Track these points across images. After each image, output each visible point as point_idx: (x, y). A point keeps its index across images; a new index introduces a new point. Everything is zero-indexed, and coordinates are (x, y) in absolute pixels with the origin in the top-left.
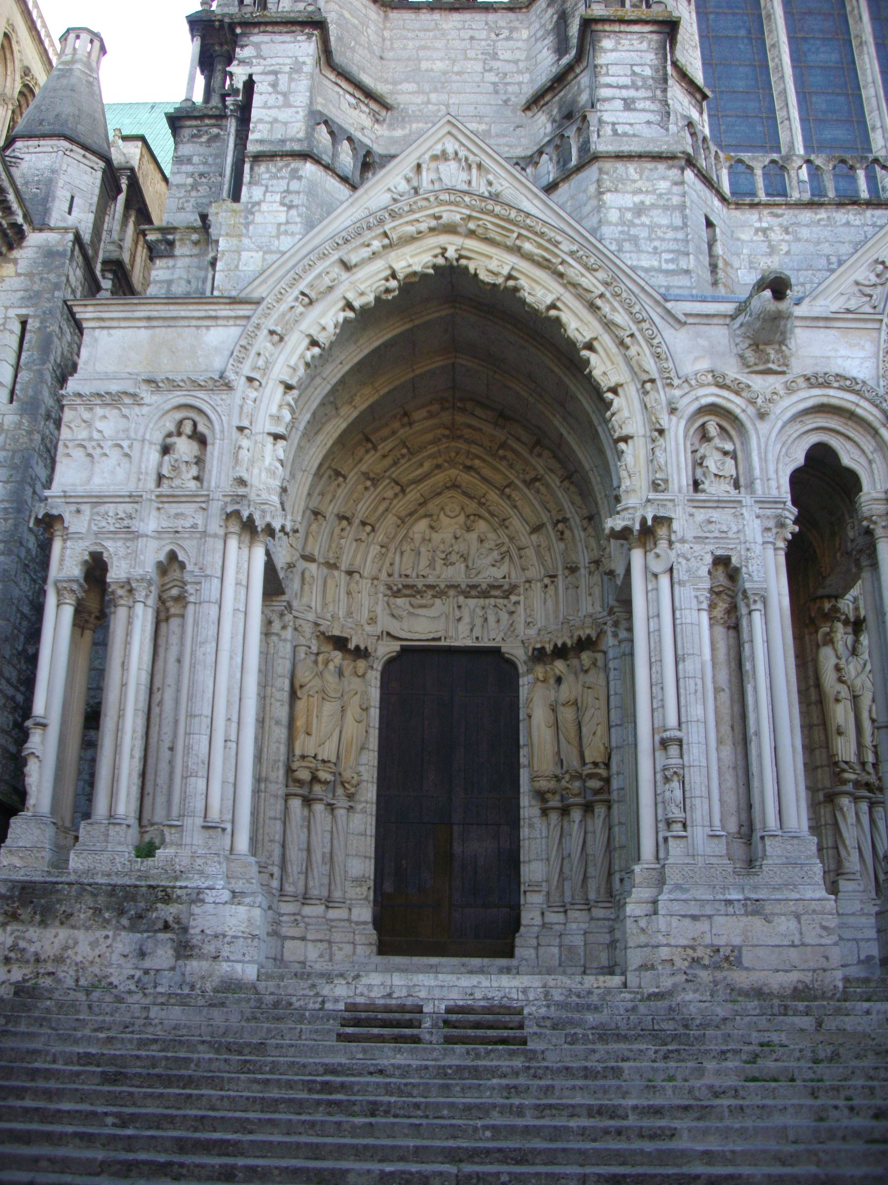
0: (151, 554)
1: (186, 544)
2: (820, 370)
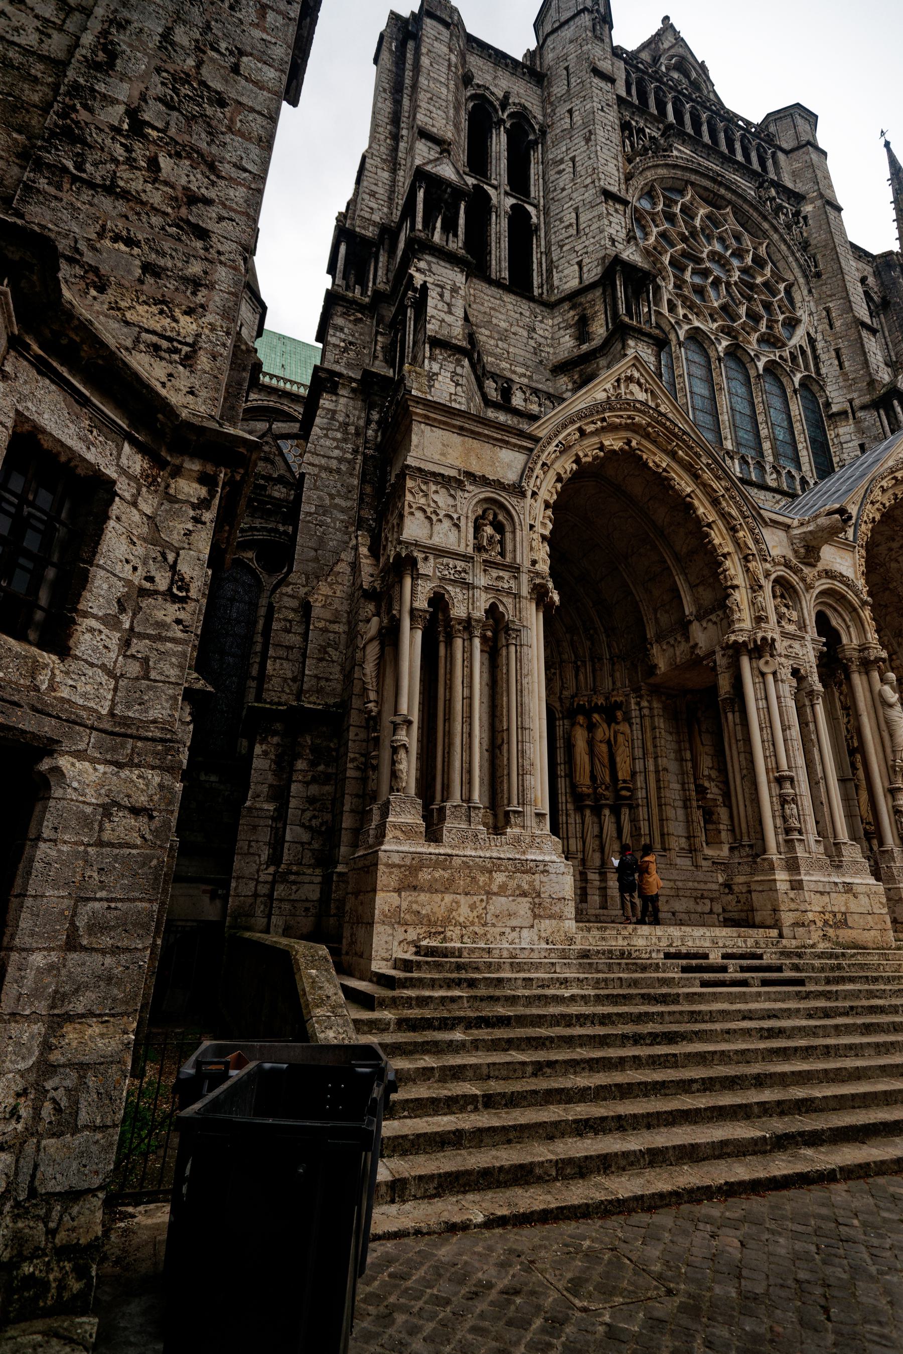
0: (483, 602)
1: (505, 600)
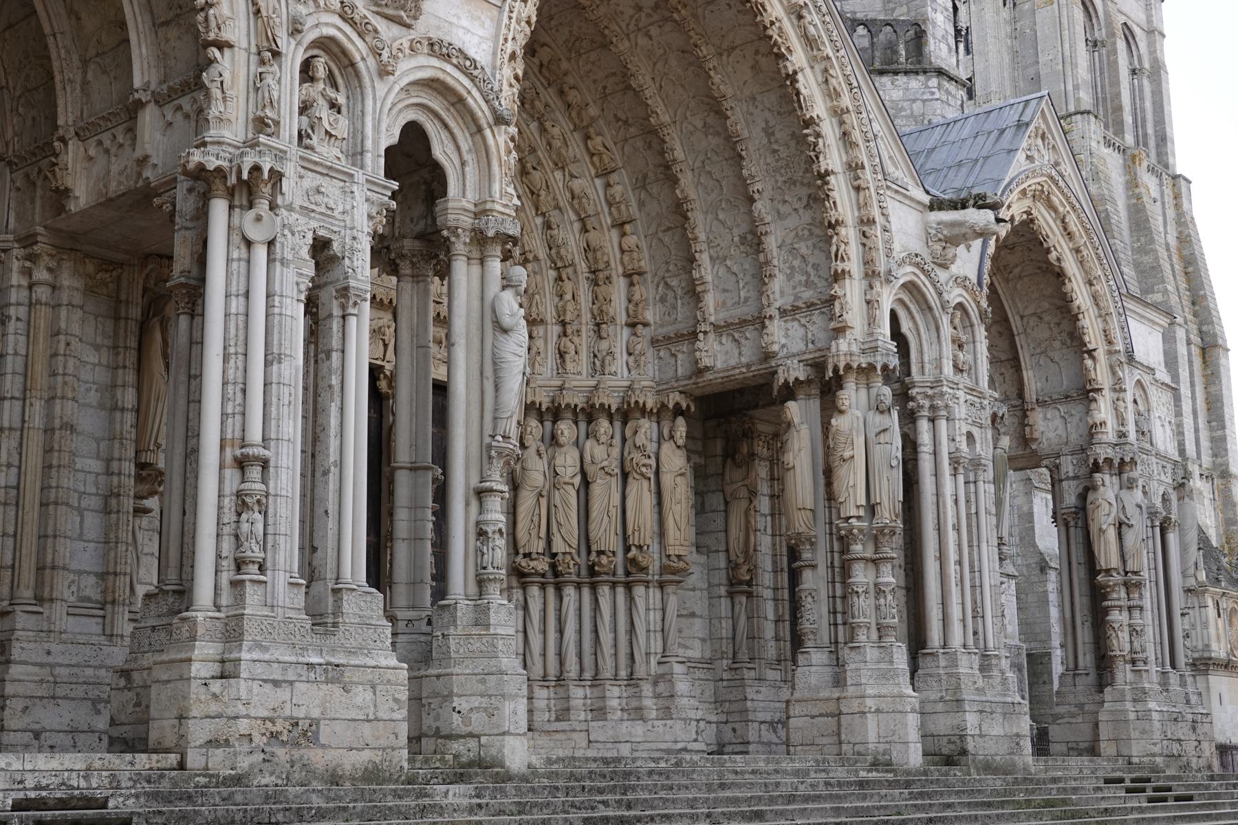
2: (447, 39)
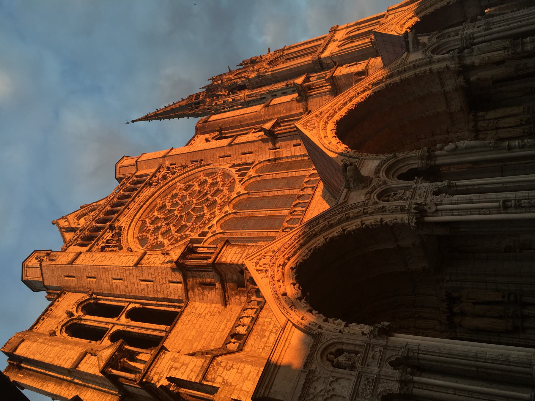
0: (388, 370)
1: (388, 356)
